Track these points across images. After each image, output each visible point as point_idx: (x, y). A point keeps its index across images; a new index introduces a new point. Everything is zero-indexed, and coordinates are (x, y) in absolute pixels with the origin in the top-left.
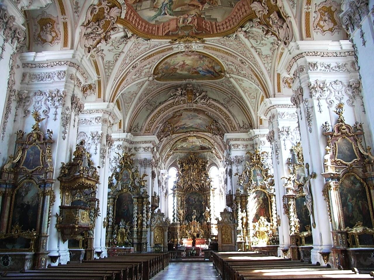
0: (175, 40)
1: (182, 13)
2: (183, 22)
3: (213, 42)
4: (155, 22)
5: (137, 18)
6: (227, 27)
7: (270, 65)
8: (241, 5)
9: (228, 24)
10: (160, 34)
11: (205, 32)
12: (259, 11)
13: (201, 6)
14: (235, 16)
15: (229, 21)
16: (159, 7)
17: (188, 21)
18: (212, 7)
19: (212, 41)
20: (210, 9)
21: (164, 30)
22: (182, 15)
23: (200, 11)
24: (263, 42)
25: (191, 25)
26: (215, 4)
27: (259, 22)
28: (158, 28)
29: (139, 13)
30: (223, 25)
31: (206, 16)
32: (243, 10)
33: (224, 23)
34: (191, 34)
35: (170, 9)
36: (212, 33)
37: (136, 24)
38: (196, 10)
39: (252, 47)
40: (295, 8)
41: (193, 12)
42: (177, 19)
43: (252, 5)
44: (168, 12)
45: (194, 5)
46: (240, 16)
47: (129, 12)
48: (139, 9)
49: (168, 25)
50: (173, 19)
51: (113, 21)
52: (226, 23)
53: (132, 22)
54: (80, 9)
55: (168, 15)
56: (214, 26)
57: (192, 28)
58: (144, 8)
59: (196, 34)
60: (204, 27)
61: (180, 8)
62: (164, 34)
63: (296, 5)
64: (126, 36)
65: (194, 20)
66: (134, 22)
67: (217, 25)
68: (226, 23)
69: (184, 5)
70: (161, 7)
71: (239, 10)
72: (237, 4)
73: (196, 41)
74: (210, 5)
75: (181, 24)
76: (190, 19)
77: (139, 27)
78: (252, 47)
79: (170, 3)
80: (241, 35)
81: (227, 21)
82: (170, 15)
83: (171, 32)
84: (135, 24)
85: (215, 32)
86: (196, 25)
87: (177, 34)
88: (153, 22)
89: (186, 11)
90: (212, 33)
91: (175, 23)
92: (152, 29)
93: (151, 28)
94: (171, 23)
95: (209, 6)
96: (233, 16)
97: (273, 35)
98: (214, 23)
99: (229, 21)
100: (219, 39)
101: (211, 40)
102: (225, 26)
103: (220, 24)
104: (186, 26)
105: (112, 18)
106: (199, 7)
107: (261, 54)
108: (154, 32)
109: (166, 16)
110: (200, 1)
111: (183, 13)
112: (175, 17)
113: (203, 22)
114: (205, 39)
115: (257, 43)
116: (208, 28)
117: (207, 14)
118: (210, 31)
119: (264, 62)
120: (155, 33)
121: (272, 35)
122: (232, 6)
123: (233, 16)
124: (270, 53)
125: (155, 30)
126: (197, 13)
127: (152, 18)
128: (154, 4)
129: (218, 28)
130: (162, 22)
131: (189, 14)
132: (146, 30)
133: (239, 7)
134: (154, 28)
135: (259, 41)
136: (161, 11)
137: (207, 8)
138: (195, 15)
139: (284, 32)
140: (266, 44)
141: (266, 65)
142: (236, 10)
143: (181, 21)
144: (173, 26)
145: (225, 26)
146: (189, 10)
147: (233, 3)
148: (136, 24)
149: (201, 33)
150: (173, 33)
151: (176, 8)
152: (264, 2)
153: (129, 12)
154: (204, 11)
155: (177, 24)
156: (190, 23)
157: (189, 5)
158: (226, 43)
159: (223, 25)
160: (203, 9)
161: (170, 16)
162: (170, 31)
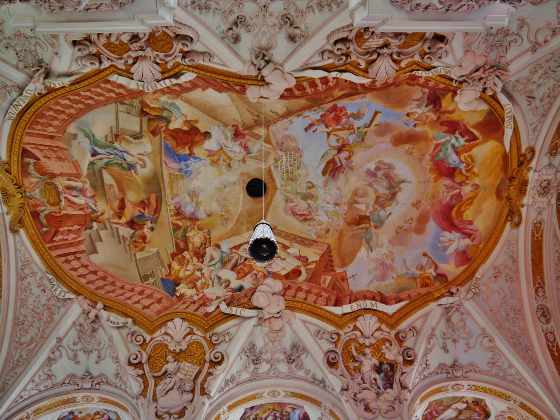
0: (8, 171)
1: (98, 186)
2: (69, 188)
3: (16, 250)
4: (74, 132)
5: (95, 101)
6: (83, 276)
7: (34, 392)
8: (157, 296)
9: (92, 277)
10: (27, 139)
11: (46, 232)
12: (166, 333)
13: (124, 220)
14: (122, 288)
15: (104, 278)
16: (116, 145)
17: (74, 196)
18: (127, 243)
19: (23, 249)
20: (121, 239)
21: (42, 148)
22: (94, 187)
23: (108, 219)
24: (81, 356)
25: (63, 203)
26: (136, 247)
27: (145, 340)
28: (52, 137)
29: (112, 107)
30: (86, 266)
31: (97, 230)
32: (147, 302)
33: (91, 268)
34: (31, 202)
35: (107, 165)
36: (49, 245)
37: (77, 98)
38: (109, 213)
39: (60, 340)
40: (219, 395)
41: (101, 206)
42: (78, 176)
43: (178, 321)
44: (101, 159)
45: (122, 207)
46: (130, 298)
47: (121, 91)
48: (122, 108)
49: (59, 158)
50: (76, 165)
51: (123, 61)
52: (95, 273)
53: (89, 90)
54: (197, 13)
55: (89, 158)
56: (73, 250)
57: (53, 205)
58: (120, 118)
59: (35, 215)
60: (61, 230)
61: (114, 183)
62: (28, 147)
63: (222, 393)
64: (48, 74)
65: (81, 209)
66: (88, 94)
67: (78, 256)
68: (95, 273)
69: (121, 189)
70: (116, 149)
71: (141, 293)
72: (155, 288)
73: (8, 213)
74: (131, 237)
75: (61, 183)
76: (81, 201)
77: (67, 102)
78: (60, 340)
79: (125, 165)
80: (75, 310)
81: (101, 274)
82: (92, 163)
83: (32, 161)
84: (79, 95)
85: (54, 253)
86: (64, 212)
87: (25, 172)
88: (72, 129)
89: (105, 195)
90: (49, 245)
91: (65, 171)
92: (51, 125)
93: (56, 123)
94: (65, 164)
95: (127, 236)
96: (119, 284)
97: (139, 379)
98: (82, 247)
99: (104, 278)
100: (34, 262)
101: (24, 245)
102: (82, 271)
103: (84, 261)
104: (59, 193)
105: (130, 62)
106: (120, 218)
107: (52, 362)
108: (39, 127)
109: (89, 155)
110: (135, 220)
111: (100, 189)
112: (85, 172)
113: (76, 227)
114: (22, 232)
115: (73, 347)
116: (60, 237)
117: (103, 233)
118: (52, 241)
119: (36, 379)
120: (34, 129)
121: (138, 376)
122: (145, 278)
123: (119, 284)
124: (60, 378)
125: (46, 131)
126: (102, 214)
127: (84, 128)
128: (128, 137)
129: (70, 258)
130: (70, 145)
131: (96, 198)
132: (51, 113)
133: (148, 292)
134: (51, 129)
135: (79, 346)
136: (102, 147)
137: (121, 233)
138: (94, 211)
139: (179, 403)
140: (78, 363)
141: (31, 385)
142: (138, 289)
143: (73, 184)
144: (54, 166)
145: (82, 271)
146: (107, 201)
147: (151, 280)
148: (77, 98)
149: (41, 223)
150: (31, 167)
151: (113, 176)
152: (193, 338)
153: (121, 91)
154: (112, 228)
155: (61, 175)
156: (69, 201)
157: (122, 200)
158: (29, 279)
159: (86, 266)
160: (114, 225)
161: (87, 163)
162: (38, 159)
